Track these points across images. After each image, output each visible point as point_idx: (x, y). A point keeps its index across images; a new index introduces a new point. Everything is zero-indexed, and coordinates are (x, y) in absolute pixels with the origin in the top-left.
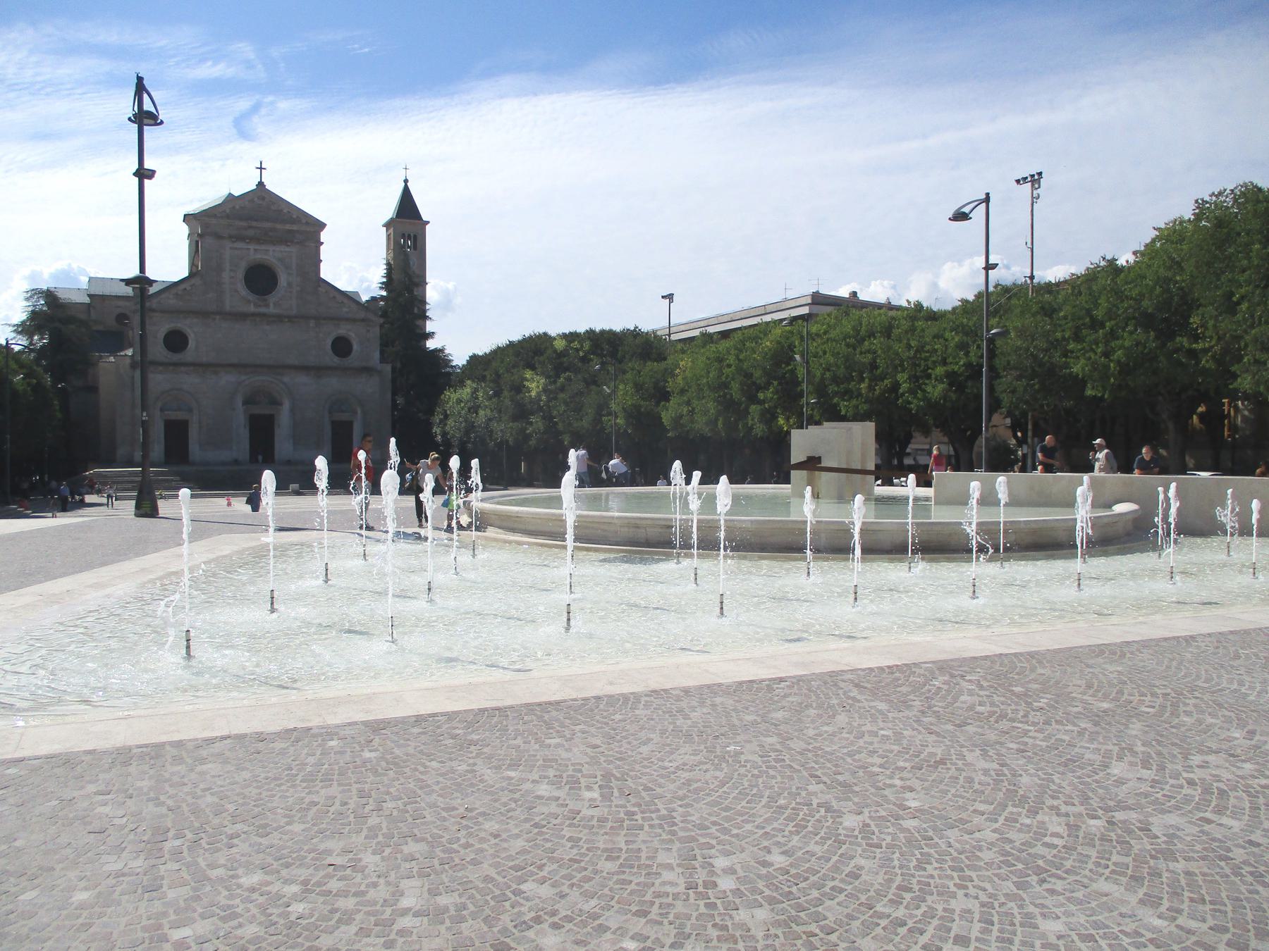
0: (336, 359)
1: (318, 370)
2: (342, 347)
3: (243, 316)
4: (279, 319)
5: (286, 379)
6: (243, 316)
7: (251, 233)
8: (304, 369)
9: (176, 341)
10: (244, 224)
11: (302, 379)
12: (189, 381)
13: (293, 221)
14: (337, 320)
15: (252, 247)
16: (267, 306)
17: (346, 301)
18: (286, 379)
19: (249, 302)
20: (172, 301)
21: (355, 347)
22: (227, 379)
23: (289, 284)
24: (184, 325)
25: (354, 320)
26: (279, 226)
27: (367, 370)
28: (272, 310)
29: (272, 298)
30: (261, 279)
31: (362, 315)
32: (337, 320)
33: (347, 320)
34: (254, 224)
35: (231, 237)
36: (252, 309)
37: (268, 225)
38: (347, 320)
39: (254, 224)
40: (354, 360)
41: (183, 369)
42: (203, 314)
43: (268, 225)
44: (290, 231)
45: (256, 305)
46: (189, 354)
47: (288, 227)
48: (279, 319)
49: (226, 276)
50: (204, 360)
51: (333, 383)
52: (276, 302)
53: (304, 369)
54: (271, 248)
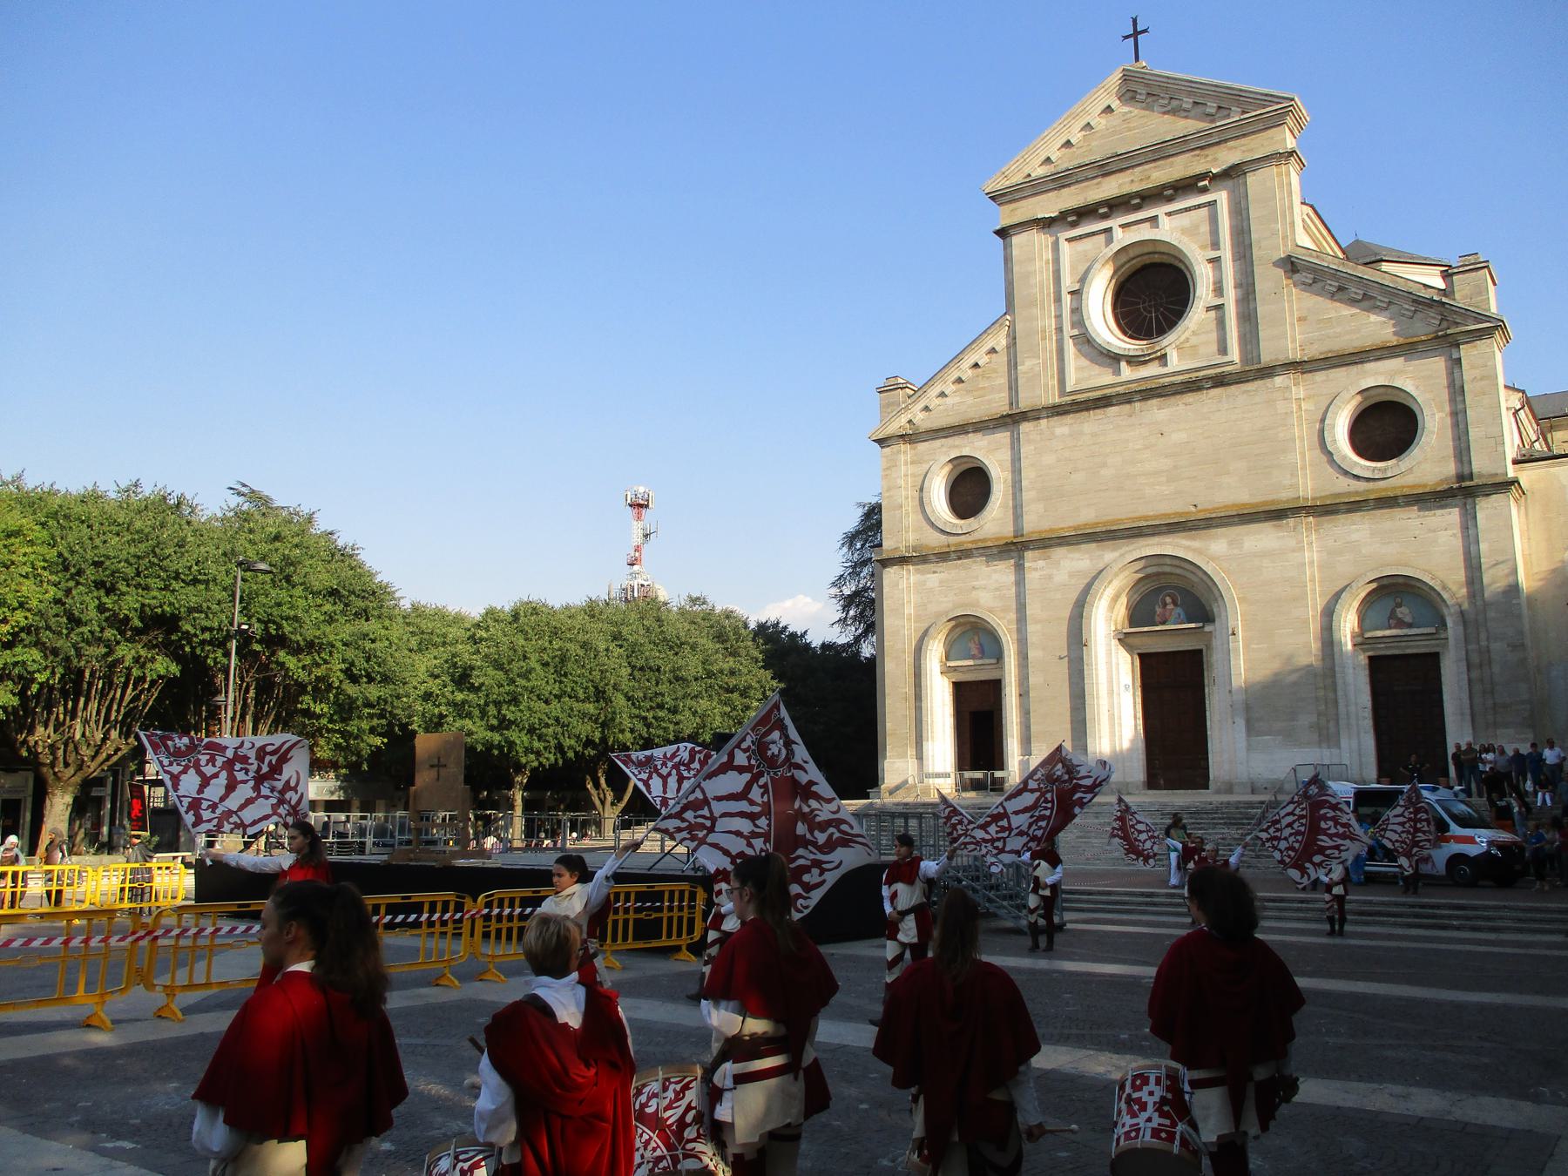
0: (1363, 466)
2: (1386, 426)
3: (1103, 402)
4: (1191, 386)
11: (1261, 538)
12: (986, 589)
15: (1114, 223)
16: (1163, 359)
19: (1113, 359)
22: (1073, 564)
23: (1219, 290)
24: (979, 447)
27: (1464, 491)
29: (1170, 342)
30: (1153, 292)
35: (1063, 215)
40: (1427, 461)
45: (1133, 361)
46: (994, 520)
48: (1191, 386)
52: (1190, 343)
54: (1160, 211)
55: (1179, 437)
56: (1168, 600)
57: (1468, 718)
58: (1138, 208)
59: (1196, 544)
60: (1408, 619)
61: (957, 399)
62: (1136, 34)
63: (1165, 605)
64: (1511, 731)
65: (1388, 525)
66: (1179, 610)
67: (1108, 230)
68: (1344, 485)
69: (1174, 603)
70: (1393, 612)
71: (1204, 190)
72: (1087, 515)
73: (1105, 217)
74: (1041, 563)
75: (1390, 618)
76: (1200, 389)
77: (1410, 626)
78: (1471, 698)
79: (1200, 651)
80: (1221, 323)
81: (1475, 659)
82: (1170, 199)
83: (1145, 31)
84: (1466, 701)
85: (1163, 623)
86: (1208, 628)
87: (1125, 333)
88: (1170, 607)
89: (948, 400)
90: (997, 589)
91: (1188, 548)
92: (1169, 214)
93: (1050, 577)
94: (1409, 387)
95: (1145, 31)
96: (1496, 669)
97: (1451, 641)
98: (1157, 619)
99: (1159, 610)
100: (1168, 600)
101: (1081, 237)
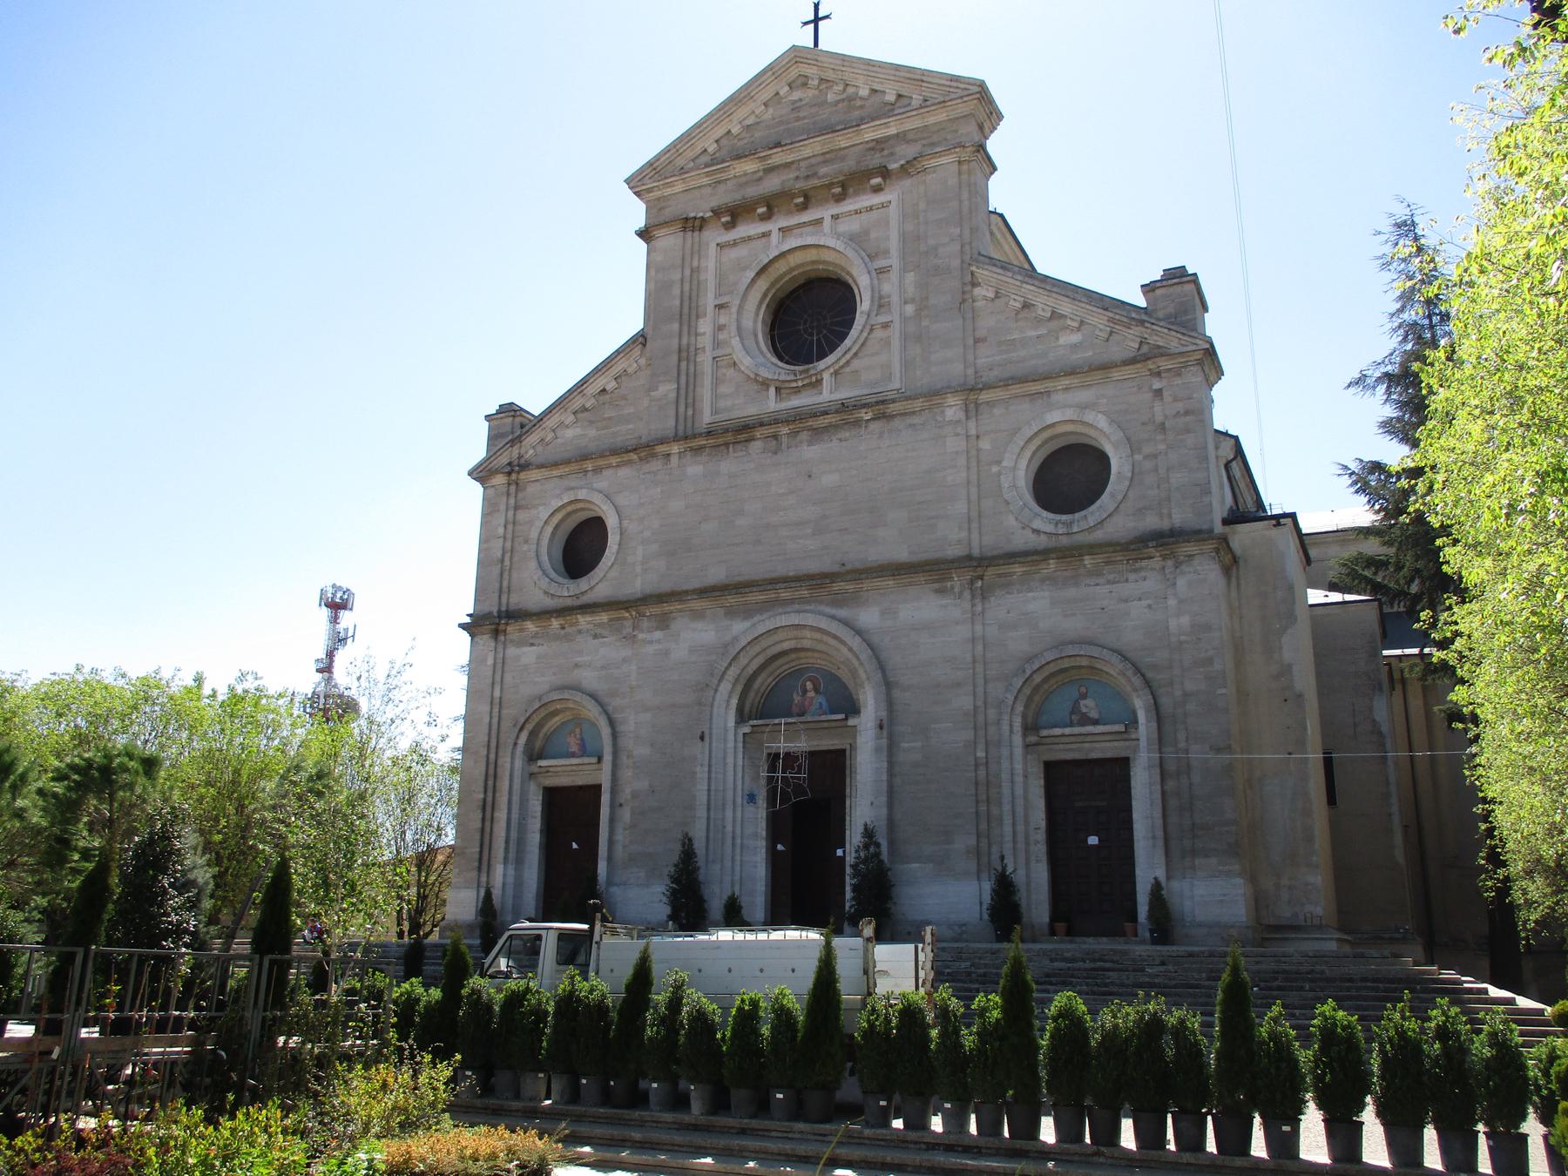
0: (1045, 521)
1: (978, 570)
4: (847, 414)
5: (868, 617)
6: (741, 432)
7: (773, 184)
8: (932, 570)
9: (581, 547)
10: (749, 166)
11: (921, 608)
13: (888, 110)
14: (1033, 381)
17: (1066, 307)
18: (868, 617)
20: (573, 435)
21: (1118, 463)
22: (696, 637)
23: (881, 304)
25: (1105, 367)
26: (842, 141)
28: (828, 394)
31: (1129, 340)
32: (1033, 381)
33: (1072, 372)
34: (779, 157)
35: (717, 213)
36: (772, 404)
37: (813, 148)
38: (1072, 372)
39: (779, 157)
41: (583, 620)
42: (644, 450)
43: (813, 148)
44: (879, 144)
47: (870, 133)
48: (847, 414)
49: (705, 326)
50: (637, 586)
51: (1037, 614)
53: (932, 570)
54: (826, 212)
55: (830, 479)
56: (809, 685)
57: (1160, 843)
58: (804, 207)
59: (842, 613)
60: (1094, 714)
61: (578, 431)
62: (816, 20)
63: (805, 691)
64: (1214, 861)
65: (1071, 592)
66: (821, 699)
67: (766, 235)
68: (1023, 539)
69: (816, 690)
70: (1076, 702)
71: (877, 189)
72: (716, 575)
73: (766, 218)
74: (658, 634)
75: (1072, 713)
76: (857, 423)
77: (1095, 722)
78: (1164, 816)
79: (841, 753)
80: (887, 343)
81: (1171, 767)
82: (839, 199)
83: (827, 17)
84: (1159, 822)
85: (802, 715)
86: (851, 722)
87: (781, 359)
88: (811, 694)
89: (569, 433)
90: (603, 668)
91: (833, 617)
92: (835, 217)
93: (667, 653)
94: (1102, 422)
95: (827, 17)
96: (1196, 778)
97: (1143, 743)
98: (795, 709)
99: (797, 698)
100: (809, 685)
101: (735, 244)
